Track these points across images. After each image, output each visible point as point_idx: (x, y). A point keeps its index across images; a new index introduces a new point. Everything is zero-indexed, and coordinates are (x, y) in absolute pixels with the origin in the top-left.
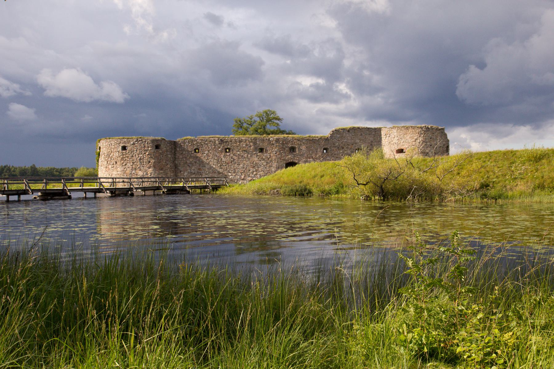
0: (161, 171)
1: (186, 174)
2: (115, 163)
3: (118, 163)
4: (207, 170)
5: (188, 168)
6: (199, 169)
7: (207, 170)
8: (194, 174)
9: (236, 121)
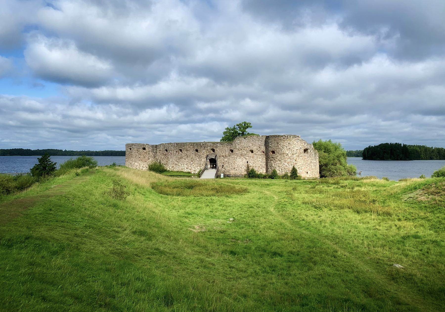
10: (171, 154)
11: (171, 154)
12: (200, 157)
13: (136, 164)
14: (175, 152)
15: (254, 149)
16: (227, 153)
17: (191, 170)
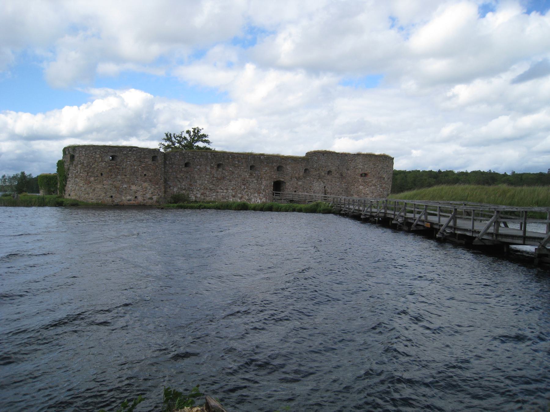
0: (157, 186)
1: (175, 189)
2: (100, 175)
3: (104, 175)
4: (198, 185)
5: (178, 183)
6: (190, 185)
7: (198, 185)
8: (185, 189)
9: (167, 135)
10: (201, 171)
11: (201, 171)
12: (259, 178)
13: (134, 188)
14: (208, 168)
15: (333, 169)
16: (301, 174)
17: (241, 198)
